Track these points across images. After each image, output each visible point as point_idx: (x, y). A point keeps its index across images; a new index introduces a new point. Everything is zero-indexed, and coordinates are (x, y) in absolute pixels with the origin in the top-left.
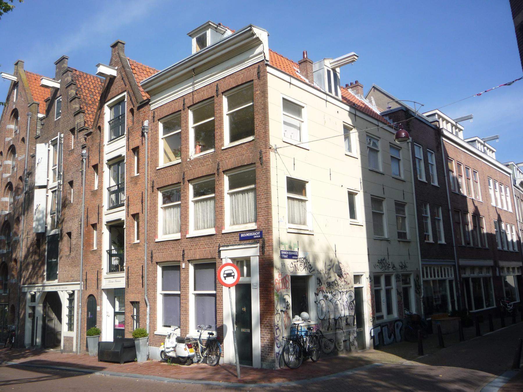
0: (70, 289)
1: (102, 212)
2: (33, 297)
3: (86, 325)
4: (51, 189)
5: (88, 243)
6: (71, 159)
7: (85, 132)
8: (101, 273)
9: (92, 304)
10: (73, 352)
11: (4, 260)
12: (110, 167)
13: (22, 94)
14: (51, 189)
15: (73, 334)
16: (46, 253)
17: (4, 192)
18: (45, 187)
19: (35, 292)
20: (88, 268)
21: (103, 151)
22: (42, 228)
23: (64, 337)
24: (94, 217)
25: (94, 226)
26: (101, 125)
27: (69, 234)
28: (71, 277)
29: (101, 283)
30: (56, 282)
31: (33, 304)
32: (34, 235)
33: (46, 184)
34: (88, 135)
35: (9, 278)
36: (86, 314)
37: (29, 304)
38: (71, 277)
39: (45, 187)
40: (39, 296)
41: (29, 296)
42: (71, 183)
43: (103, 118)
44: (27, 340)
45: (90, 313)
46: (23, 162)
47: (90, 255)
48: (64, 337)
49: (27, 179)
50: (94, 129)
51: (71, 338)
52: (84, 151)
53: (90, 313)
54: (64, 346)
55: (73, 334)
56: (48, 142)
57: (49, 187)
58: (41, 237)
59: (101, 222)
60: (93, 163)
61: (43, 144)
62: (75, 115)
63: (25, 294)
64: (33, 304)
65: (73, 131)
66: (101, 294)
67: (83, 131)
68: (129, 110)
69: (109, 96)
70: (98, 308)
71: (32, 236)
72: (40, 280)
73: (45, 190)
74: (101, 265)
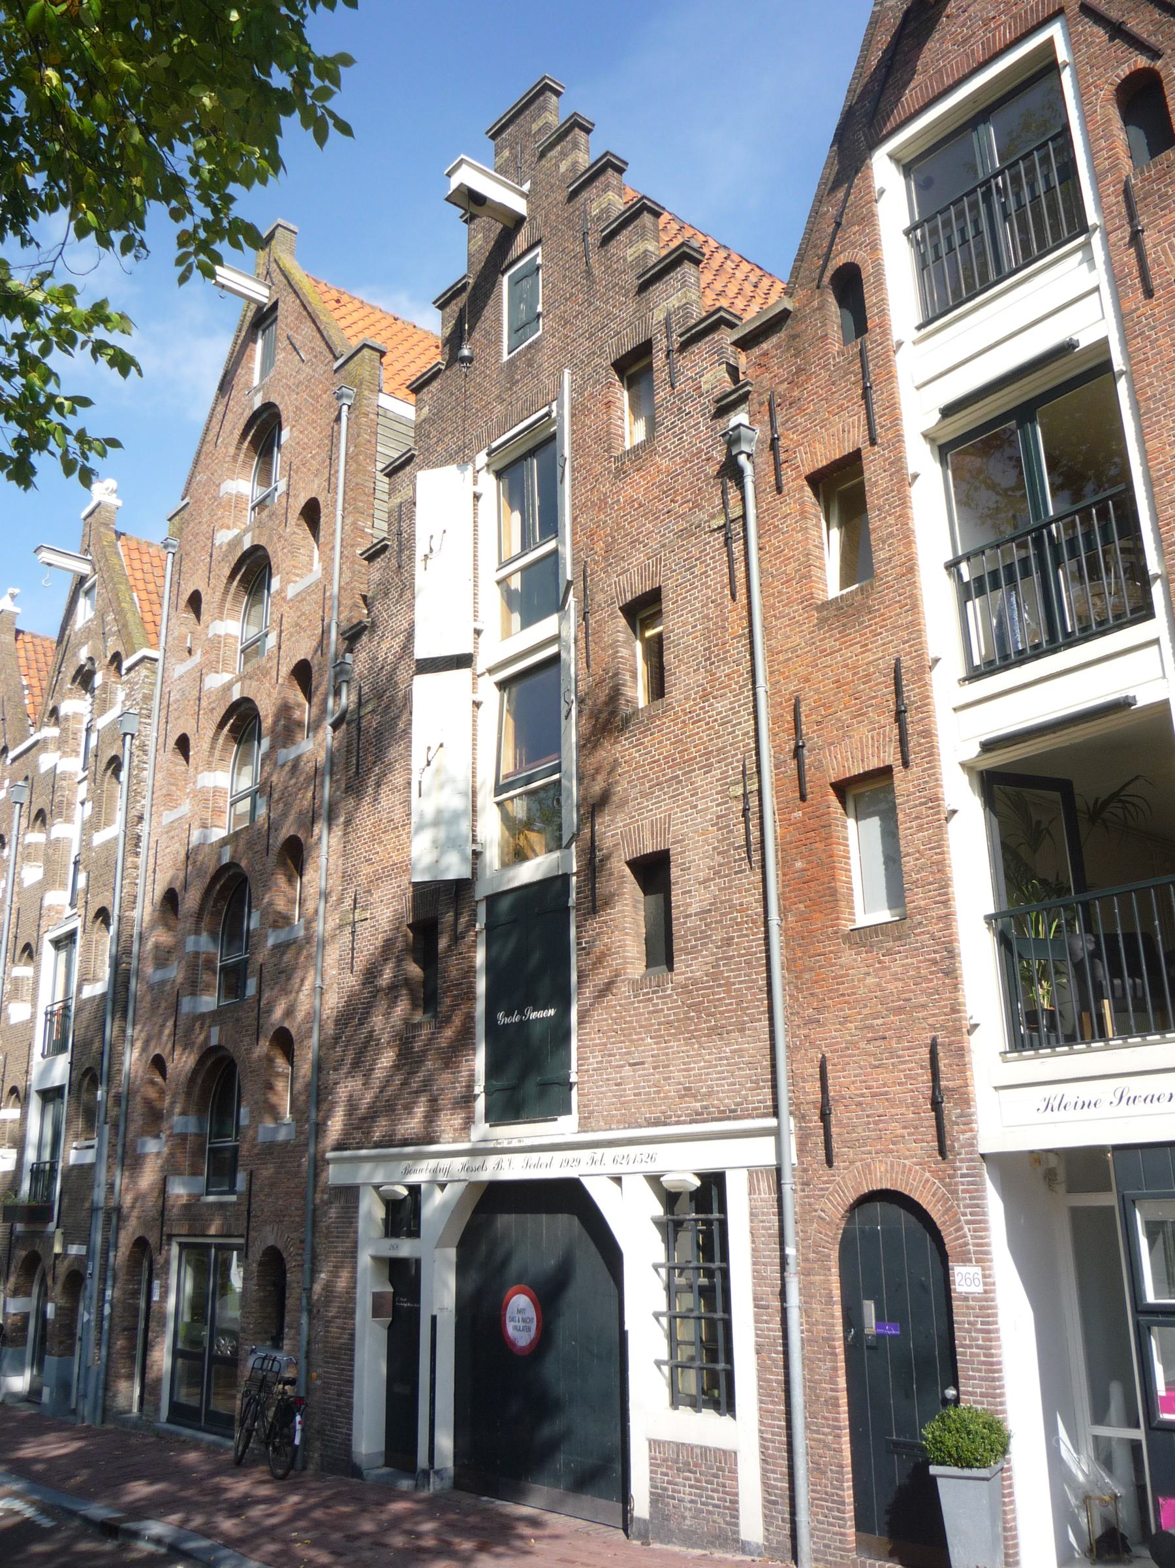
0: (683, 1165)
1: (925, 698)
2: (403, 1215)
3: (842, 1382)
4: (491, 671)
5: (818, 888)
6: (636, 487)
7: (727, 337)
8: (960, 1052)
9: (895, 1259)
10: (744, 1547)
11: (214, 1041)
12: (943, 451)
13: (298, 340)
14: (491, 671)
15: (740, 1433)
16: (481, 986)
17: (212, 748)
18: (463, 661)
19: (414, 1190)
20: (833, 1034)
21: (891, 378)
22: (464, 859)
23: (654, 1444)
24: (862, 732)
25: (867, 791)
26: (858, 256)
27: (653, 871)
28: (688, 1092)
29: (967, 1120)
30: (564, 1127)
31: (405, 1248)
32: (404, 904)
33: (468, 649)
34: (745, 343)
35: (244, 1121)
36: (838, 1311)
37: (372, 1243)
38: (688, 1092)
39: (463, 661)
40: (444, 1205)
41: (372, 1210)
42: (643, 610)
43: (868, 220)
44: (368, 1437)
45: (869, 1308)
46: (317, 597)
47: (848, 956)
48: (654, 1444)
49: (349, 658)
50: (801, 293)
51: (720, 1463)
52: (740, 417)
53: (869, 1308)
54: (656, 1499)
55: (740, 1433)
56: (472, 459)
57: (481, 664)
58: (436, 908)
59: (931, 753)
60: (823, 454)
61: (452, 469)
62: (643, 288)
63: (349, 1195)
64: (405, 1248)
65: (634, 367)
66: (977, 1195)
67: (716, 336)
68: (1106, 92)
69: (910, 96)
70: (964, 1279)
71: (386, 910)
72: (449, 1122)
73: (465, 674)
74: (955, 1009)
